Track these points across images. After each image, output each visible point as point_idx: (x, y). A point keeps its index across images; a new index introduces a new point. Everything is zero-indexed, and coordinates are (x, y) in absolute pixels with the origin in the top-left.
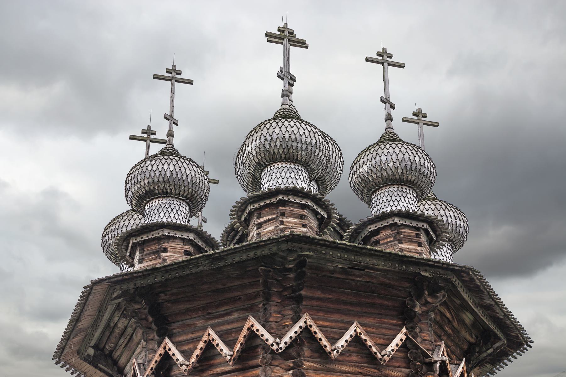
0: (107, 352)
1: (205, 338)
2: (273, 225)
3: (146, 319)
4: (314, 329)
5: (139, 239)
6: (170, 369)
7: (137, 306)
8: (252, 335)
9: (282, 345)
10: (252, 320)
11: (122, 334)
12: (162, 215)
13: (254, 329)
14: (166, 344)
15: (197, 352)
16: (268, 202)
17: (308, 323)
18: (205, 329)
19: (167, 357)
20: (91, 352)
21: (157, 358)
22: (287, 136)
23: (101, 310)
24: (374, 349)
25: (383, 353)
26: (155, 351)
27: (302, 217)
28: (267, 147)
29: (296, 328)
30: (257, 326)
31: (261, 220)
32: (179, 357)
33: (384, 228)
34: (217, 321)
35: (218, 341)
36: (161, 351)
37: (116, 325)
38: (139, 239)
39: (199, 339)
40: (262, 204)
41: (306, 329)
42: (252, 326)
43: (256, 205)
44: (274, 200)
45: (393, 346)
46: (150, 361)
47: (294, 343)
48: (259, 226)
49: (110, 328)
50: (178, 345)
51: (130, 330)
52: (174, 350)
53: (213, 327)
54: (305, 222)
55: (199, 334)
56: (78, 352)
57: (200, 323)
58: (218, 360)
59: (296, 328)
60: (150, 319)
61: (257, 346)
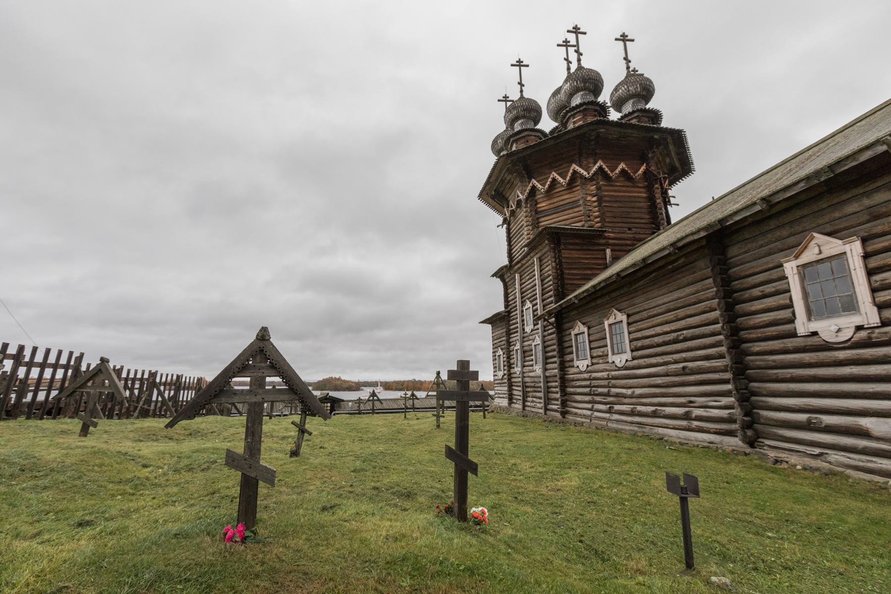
0: (500, 192)
1: (552, 176)
3: (521, 173)
4: (604, 166)
5: (515, 138)
6: (535, 193)
7: (517, 168)
8: (575, 172)
9: (590, 174)
11: (508, 183)
13: (576, 169)
15: (548, 183)
16: (578, 110)
18: (551, 173)
19: (534, 187)
20: (493, 193)
21: (529, 188)
22: (586, 76)
23: (500, 172)
24: (632, 174)
25: (637, 175)
26: (527, 186)
29: (596, 167)
31: (575, 120)
32: (539, 186)
34: (556, 169)
35: (558, 177)
36: (531, 185)
37: (505, 179)
38: (515, 138)
40: (575, 111)
41: (600, 168)
43: (572, 113)
44: (581, 108)
45: (640, 172)
46: (525, 191)
47: (595, 173)
49: (502, 181)
51: (512, 180)
53: (555, 171)
55: (547, 176)
56: (487, 194)
57: (547, 171)
58: (558, 185)
59: (596, 167)
60: (524, 172)
61: (577, 178)
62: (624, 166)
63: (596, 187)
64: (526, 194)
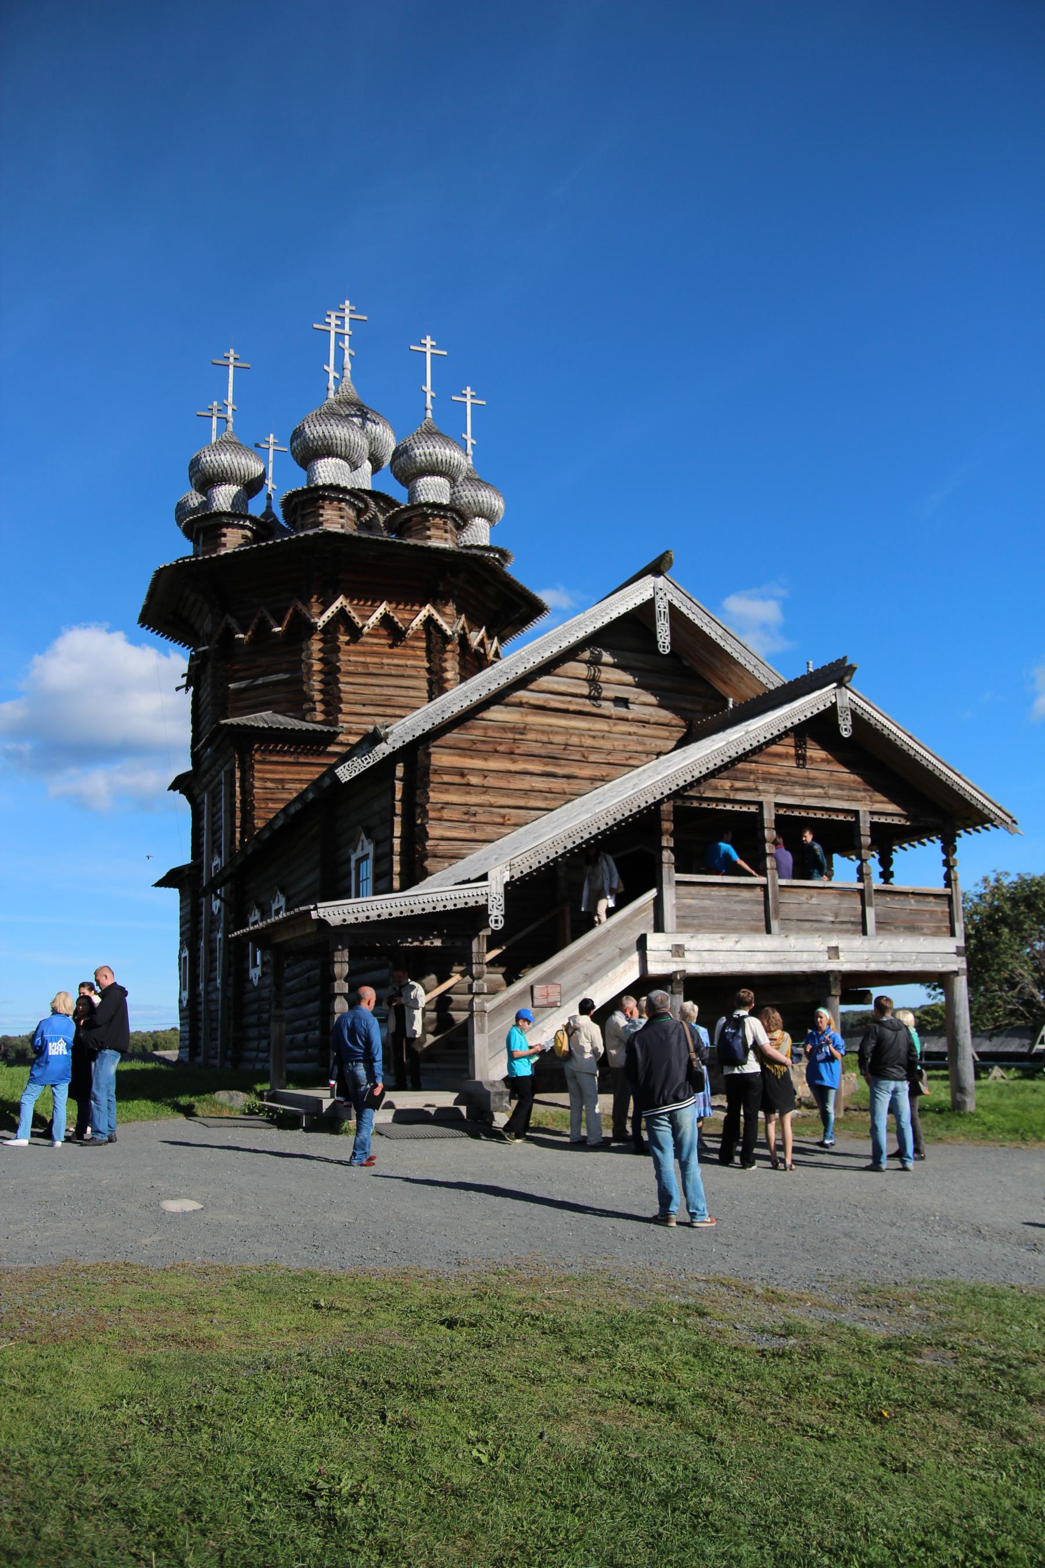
1: (259, 615)
4: (348, 609)
27: (340, 509)
31: (305, 512)
33: (415, 516)
36: (223, 625)
41: (342, 611)
54: (343, 514)
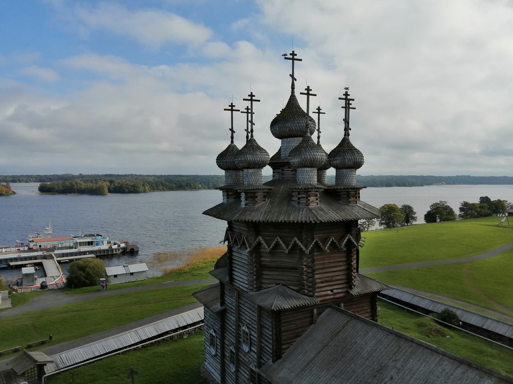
1: (276, 240)
2: (305, 200)
4: (319, 242)
10: (296, 239)
12: (253, 178)
14: (259, 238)
17: (317, 240)
18: (276, 237)
21: (256, 243)
28: (304, 163)
30: (298, 242)
31: (300, 196)
35: (281, 243)
39: (273, 240)
42: (296, 241)
48: (299, 198)
50: (265, 240)
52: (263, 242)
62: (333, 239)
63: (312, 260)
64: (252, 247)
